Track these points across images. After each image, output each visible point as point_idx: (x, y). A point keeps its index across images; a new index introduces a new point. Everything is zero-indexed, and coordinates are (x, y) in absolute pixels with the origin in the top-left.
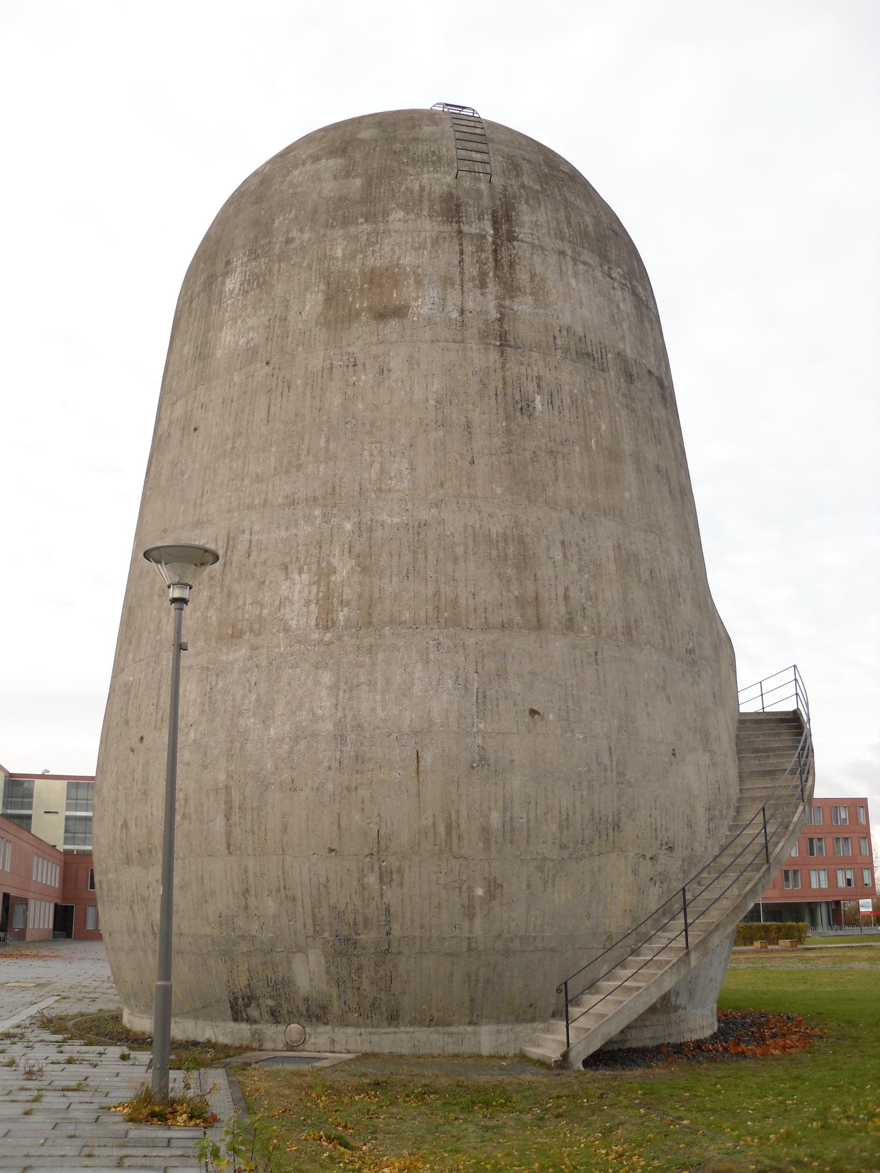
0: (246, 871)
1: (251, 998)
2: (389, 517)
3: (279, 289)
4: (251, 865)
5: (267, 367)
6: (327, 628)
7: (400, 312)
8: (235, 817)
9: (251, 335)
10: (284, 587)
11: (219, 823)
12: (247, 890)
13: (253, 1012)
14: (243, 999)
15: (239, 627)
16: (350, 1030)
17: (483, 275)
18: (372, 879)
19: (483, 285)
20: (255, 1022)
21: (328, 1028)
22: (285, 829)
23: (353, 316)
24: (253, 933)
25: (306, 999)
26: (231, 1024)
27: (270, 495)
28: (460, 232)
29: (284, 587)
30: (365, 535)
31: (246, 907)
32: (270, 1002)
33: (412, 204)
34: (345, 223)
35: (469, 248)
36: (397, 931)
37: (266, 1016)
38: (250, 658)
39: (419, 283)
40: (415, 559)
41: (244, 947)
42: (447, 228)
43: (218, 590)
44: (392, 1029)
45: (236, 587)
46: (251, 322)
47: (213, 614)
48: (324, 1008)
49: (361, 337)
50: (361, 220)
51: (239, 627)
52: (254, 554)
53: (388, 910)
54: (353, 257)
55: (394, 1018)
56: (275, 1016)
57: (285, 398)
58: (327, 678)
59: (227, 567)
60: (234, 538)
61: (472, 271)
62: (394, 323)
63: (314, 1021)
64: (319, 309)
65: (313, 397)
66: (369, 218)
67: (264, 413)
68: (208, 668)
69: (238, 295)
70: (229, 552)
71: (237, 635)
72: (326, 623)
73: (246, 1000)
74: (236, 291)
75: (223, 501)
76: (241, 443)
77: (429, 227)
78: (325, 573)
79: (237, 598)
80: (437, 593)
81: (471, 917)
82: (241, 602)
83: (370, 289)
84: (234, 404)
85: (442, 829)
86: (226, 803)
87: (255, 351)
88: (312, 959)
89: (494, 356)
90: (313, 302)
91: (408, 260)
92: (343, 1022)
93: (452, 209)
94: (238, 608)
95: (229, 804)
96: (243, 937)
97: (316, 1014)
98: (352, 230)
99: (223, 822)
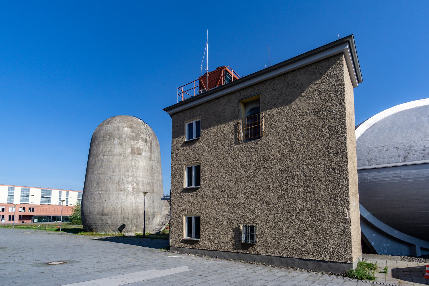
2: (140, 179)
3: (124, 147)
7: (140, 154)
10: (128, 186)
11: (120, 211)
23: (135, 153)
33: (142, 139)
34: (134, 140)
47: (118, 188)
49: (135, 156)
58: (133, 196)
66: (137, 140)
71: (121, 190)
72: (133, 190)
76: (120, 166)
77: (144, 143)
78: (133, 185)
87: (121, 154)
90: (129, 150)
91: (141, 147)
93: (146, 141)
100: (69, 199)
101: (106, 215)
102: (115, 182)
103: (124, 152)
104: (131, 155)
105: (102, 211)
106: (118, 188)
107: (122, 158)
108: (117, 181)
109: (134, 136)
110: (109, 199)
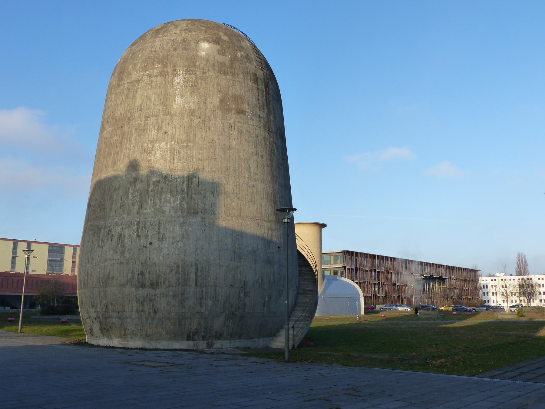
0: (202, 291)
1: (196, 333)
4: (204, 289)
5: (199, 119)
6: (228, 216)
8: (199, 273)
9: (191, 104)
11: (193, 276)
13: (196, 337)
15: (196, 210)
16: (227, 341)
17: (263, 105)
18: (242, 295)
19: (264, 109)
20: (196, 340)
21: (221, 341)
22: (217, 279)
23: (229, 110)
24: (202, 311)
26: (186, 342)
27: (205, 167)
28: (258, 88)
29: (213, 199)
30: (238, 187)
31: (201, 303)
32: (203, 334)
34: (225, 74)
35: (260, 95)
36: (247, 310)
38: (202, 221)
39: (248, 104)
40: (252, 197)
42: (254, 85)
43: (186, 196)
45: (194, 196)
46: (189, 99)
48: (221, 335)
50: (230, 75)
51: (196, 210)
52: (200, 186)
53: (245, 304)
54: (229, 88)
55: (240, 337)
56: (204, 338)
59: (189, 188)
60: (191, 179)
61: (261, 103)
62: (242, 116)
64: (218, 104)
65: (218, 135)
67: (200, 136)
68: (184, 223)
69: (182, 86)
71: (196, 213)
74: (181, 84)
75: (185, 164)
79: (195, 200)
80: (257, 209)
81: (264, 306)
82: (196, 202)
85: (260, 280)
87: (194, 111)
88: (221, 319)
89: (267, 134)
92: (225, 339)
93: (256, 80)
94: (195, 204)
95: (197, 270)
96: (198, 313)
97: (219, 337)
98: (228, 77)
99: (194, 275)
100: (32, 259)
101: (154, 285)
102: (179, 188)
103: (203, 107)
104: (219, 113)
105: (142, 274)
106: (185, 205)
107: (197, 121)
108: (185, 187)
109: (228, 64)
110: (162, 239)
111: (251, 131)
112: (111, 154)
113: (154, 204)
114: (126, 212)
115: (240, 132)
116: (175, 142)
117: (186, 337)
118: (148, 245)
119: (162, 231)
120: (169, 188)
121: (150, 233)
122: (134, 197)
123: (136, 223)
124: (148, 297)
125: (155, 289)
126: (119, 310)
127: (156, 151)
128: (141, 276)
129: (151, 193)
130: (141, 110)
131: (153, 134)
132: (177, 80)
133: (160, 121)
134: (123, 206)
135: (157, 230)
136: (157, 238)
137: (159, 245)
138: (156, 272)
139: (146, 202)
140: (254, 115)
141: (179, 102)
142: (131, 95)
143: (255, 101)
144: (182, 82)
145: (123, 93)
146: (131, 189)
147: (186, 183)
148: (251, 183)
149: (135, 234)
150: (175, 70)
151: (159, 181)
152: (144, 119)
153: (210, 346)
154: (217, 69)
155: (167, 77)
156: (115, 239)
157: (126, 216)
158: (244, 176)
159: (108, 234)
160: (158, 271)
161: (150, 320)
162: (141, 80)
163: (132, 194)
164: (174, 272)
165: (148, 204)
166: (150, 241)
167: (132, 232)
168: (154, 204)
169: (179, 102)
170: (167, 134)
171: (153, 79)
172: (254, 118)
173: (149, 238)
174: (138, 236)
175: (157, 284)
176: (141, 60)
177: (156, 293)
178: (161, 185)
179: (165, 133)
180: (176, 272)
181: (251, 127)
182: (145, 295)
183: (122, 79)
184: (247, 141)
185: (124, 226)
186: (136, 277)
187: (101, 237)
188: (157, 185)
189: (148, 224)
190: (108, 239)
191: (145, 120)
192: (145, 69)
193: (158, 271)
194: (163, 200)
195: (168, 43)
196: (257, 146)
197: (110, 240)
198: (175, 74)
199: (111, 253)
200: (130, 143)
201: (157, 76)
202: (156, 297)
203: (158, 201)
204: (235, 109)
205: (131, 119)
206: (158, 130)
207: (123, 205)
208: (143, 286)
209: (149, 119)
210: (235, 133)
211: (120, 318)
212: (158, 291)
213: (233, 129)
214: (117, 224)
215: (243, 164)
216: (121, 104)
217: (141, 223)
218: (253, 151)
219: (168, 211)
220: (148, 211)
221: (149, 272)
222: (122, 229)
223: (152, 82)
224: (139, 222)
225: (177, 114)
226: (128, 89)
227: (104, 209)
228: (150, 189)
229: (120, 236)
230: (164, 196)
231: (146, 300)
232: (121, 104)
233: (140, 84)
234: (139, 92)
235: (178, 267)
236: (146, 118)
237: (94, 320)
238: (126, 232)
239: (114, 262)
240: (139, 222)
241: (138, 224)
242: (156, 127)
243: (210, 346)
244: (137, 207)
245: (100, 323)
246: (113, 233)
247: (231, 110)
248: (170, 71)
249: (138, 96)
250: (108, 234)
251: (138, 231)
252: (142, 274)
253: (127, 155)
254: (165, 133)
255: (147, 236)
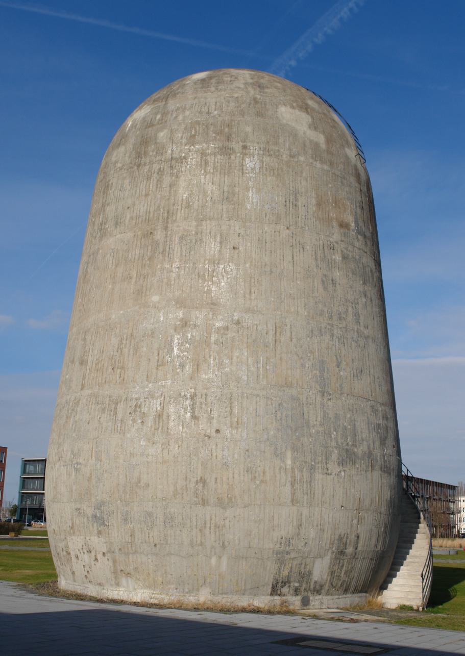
1: (286, 583)
5: (288, 231)
12: (301, 525)
13: (285, 590)
14: (282, 583)
18: (355, 522)
20: (284, 595)
21: (320, 597)
22: (323, 494)
24: (300, 547)
25: (316, 582)
31: (299, 534)
32: (297, 585)
36: (359, 549)
37: (292, 592)
41: (293, 555)
44: (345, 596)
50: (328, 164)
53: (358, 537)
56: (297, 591)
57: (301, 254)
59: (277, 343)
63: (315, 593)
65: (316, 259)
67: (290, 258)
70: (278, 335)
73: (283, 584)
74: (257, 170)
80: (370, 383)
83: (336, 207)
84: (267, 244)
86: (291, 477)
97: (318, 591)
105: (203, 481)
111: (357, 257)
112: (131, 278)
113: (221, 365)
114: (169, 376)
115: (345, 258)
116: (251, 265)
117: (270, 591)
118: (213, 433)
119: (236, 411)
120: (245, 340)
121: (215, 413)
122: (183, 351)
123: (189, 396)
124: (213, 521)
125: (224, 508)
126: (157, 542)
127: (220, 277)
128: (200, 486)
129: (213, 346)
130: (188, 206)
131: (212, 247)
132: (249, 163)
133: (224, 227)
134: (163, 365)
135: (228, 409)
136: (228, 422)
137: (232, 435)
138: (228, 479)
139: (205, 361)
140: (359, 232)
141: (255, 200)
142: (167, 180)
143: (359, 210)
144: (257, 167)
145: (149, 178)
146: (176, 337)
147: (271, 333)
148: (362, 342)
149: (189, 414)
150: (245, 147)
151: (227, 328)
152: (194, 223)
153: (305, 602)
154: (310, 152)
155: (233, 157)
156: (150, 421)
157: (169, 382)
158: (353, 330)
159: (135, 411)
160: (231, 479)
161: (214, 561)
162: (185, 158)
163: (180, 345)
164: (258, 482)
165: (209, 365)
166: (215, 425)
167: (182, 411)
168: (221, 365)
169: (255, 200)
170: (236, 251)
171: (208, 158)
172: (359, 237)
173: (215, 421)
174: (194, 417)
175: (230, 499)
176: (183, 126)
177: (227, 514)
178: (230, 334)
179: (234, 248)
180: (262, 481)
181: (357, 251)
182: (208, 518)
183: (146, 153)
184: (354, 274)
185: (167, 399)
186: (192, 485)
187: (120, 416)
188: (224, 334)
189: (209, 399)
190: (134, 421)
191: (197, 226)
192: (192, 140)
193: (231, 479)
194: (235, 358)
195: (229, 102)
196: (364, 283)
197: (140, 421)
198: (246, 154)
199: (142, 443)
200: (171, 261)
201: (215, 154)
202: (227, 521)
203: (226, 361)
204: (337, 219)
205: (170, 220)
206: (221, 243)
207: (160, 364)
208: (204, 503)
209: (204, 223)
210: (338, 257)
211: (156, 555)
212: (229, 513)
213: (335, 251)
214: (151, 395)
215: (350, 309)
216: (147, 195)
217: (199, 396)
218: (361, 289)
219: (245, 378)
220: (211, 376)
221: (216, 479)
222: (163, 405)
223: (206, 163)
224: (195, 394)
225: (253, 218)
226: (161, 172)
227: (123, 368)
228: (213, 339)
229: (160, 416)
230: (236, 354)
231: (208, 526)
232: (147, 195)
233: (184, 164)
234: (182, 178)
235: (264, 473)
236: (200, 221)
237: (100, 556)
238: (172, 409)
239: (149, 460)
240: (195, 394)
241: (192, 398)
242: (218, 238)
243: (305, 602)
244: (188, 368)
245: (114, 562)
246: (144, 409)
247: (332, 221)
248: (237, 146)
249: (182, 183)
250: (135, 411)
251: (193, 408)
252: (203, 481)
253: (165, 280)
254: (234, 248)
255: (210, 419)
